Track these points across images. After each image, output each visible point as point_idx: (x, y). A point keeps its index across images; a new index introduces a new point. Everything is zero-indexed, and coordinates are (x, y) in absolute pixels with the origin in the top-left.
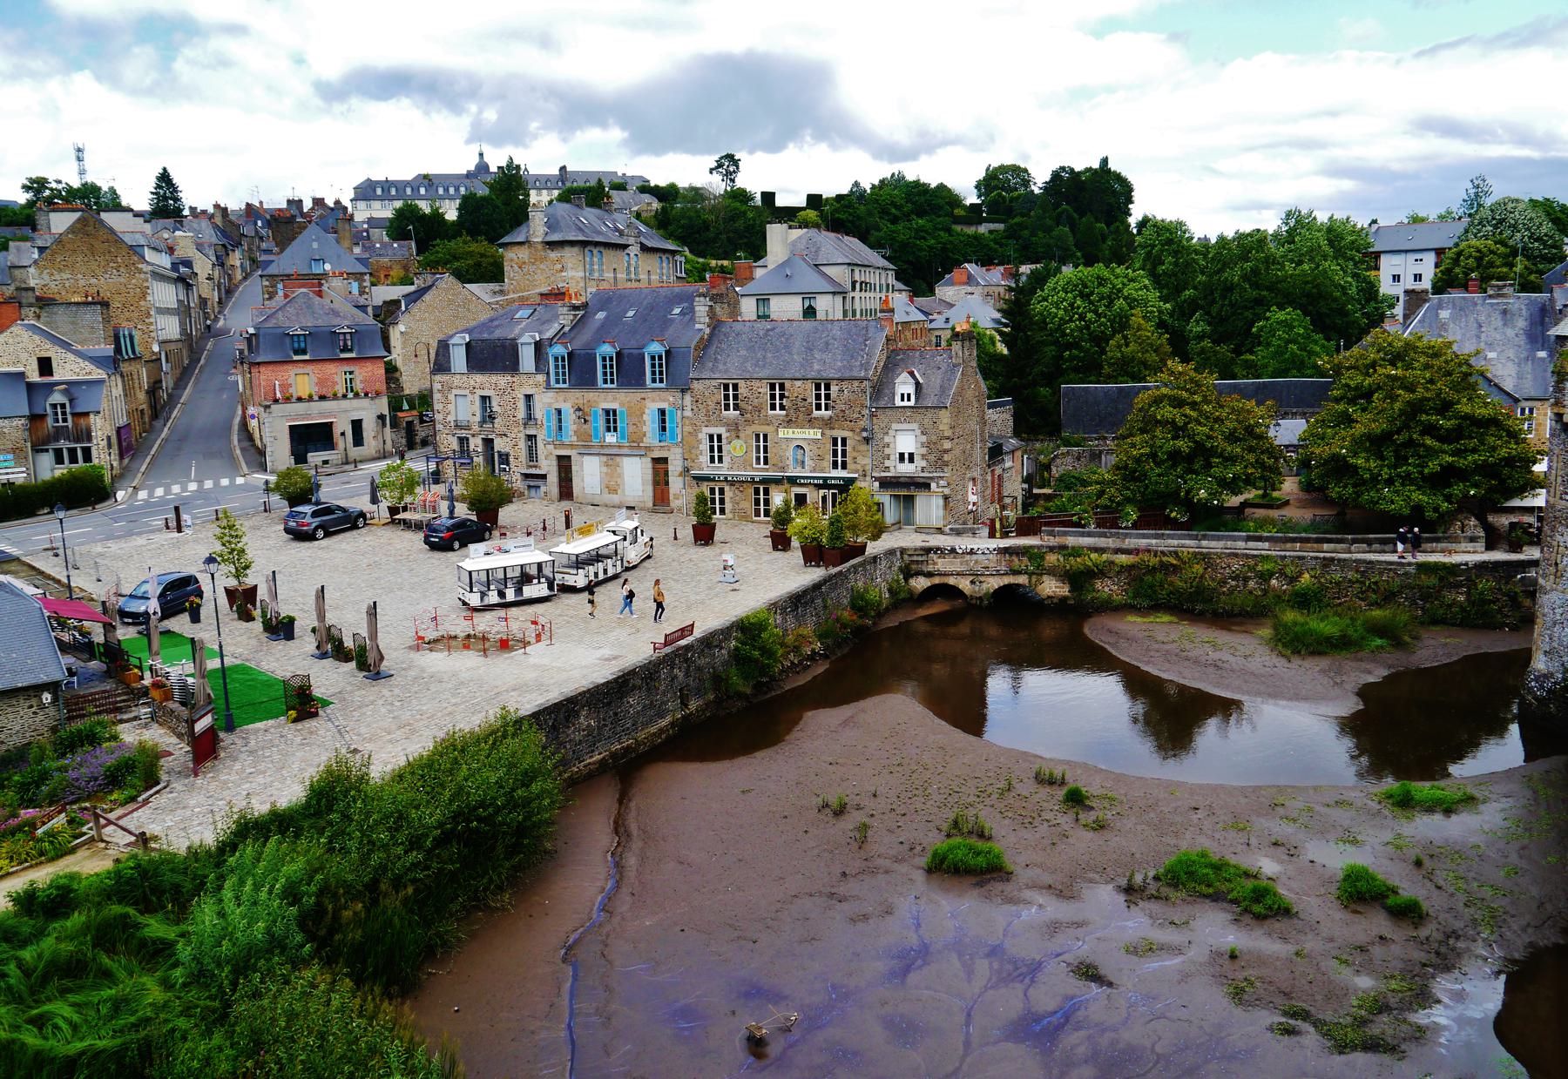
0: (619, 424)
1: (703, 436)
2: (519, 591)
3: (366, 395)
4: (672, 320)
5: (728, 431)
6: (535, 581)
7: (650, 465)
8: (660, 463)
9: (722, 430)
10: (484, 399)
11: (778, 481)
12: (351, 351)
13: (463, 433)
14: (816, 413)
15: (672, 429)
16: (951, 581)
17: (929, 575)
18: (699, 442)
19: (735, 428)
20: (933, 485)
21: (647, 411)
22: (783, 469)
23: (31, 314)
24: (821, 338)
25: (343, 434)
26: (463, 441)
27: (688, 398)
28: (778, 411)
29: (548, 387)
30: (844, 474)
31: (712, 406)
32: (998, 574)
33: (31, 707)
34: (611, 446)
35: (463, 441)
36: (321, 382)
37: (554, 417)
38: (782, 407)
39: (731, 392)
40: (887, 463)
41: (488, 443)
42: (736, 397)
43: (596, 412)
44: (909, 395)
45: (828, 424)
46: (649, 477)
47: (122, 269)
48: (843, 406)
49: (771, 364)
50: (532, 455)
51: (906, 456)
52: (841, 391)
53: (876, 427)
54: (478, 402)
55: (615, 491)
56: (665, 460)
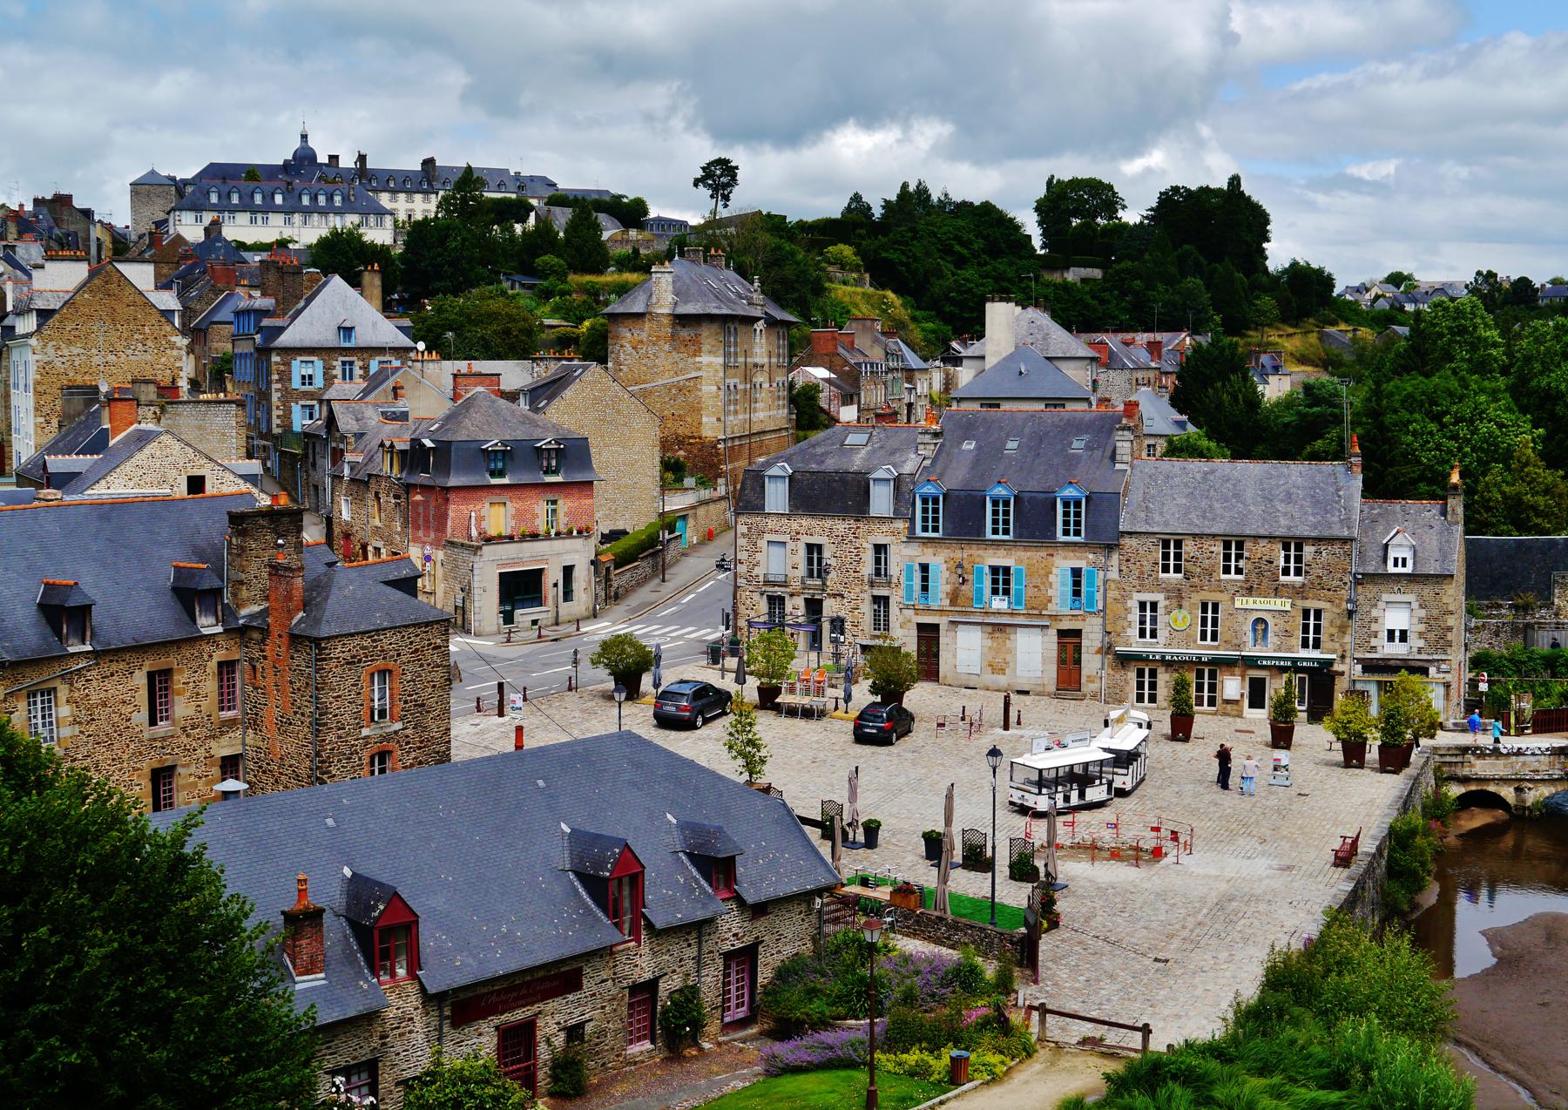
0: (1013, 586)
1: (1133, 604)
2: (1082, 795)
3: (580, 532)
4: (1077, 458)
5: (1167, 598)
6: (1097, 782)
7: (1055, 639)
8: (1070, 639)
9: (1159, 597)
10: (811, 548)
11: (1228, 664)
12: (555, 472)
13: (779, 591)
14: (1282, 578)
15: (1091, 596)
16: (1492, 788)
17: (1465, 780)
18: (1128, 611)
19: (1177, 596)
20: (1432, 670)
21: (1054, 570)
22: (1238, 647)
23: (150, 415)
24: (1278, 486)
25: (556, 585)
26: (776, 602)
27: (1115, 557)
28: (1233, 576)
29: (912, 537)
30: (1316, 654)
31: (1147, 567)
32: (1552, 781)
33: (801, 913)
34: (999, 613)
35: (776, 602)
36: (519, 516)
37: (917, 576)
38: (1239, 571)
39: (1172, 551)
40: (1374, 642)
41: (814, 606)
42: (1178, 557)
43: (981, 571)
44: (1404, 560)
45: (1299, 592)
46: (1055, 654)
47: (149, 343)
48: (1320, 572)
49: (1222, 517)
50: (881, 620)
51: (1397, 634)
52: (1318, 552)
53: (1361, 598)
54: (802, 553)
55: (1002, 671)
56: (1077, 633)
